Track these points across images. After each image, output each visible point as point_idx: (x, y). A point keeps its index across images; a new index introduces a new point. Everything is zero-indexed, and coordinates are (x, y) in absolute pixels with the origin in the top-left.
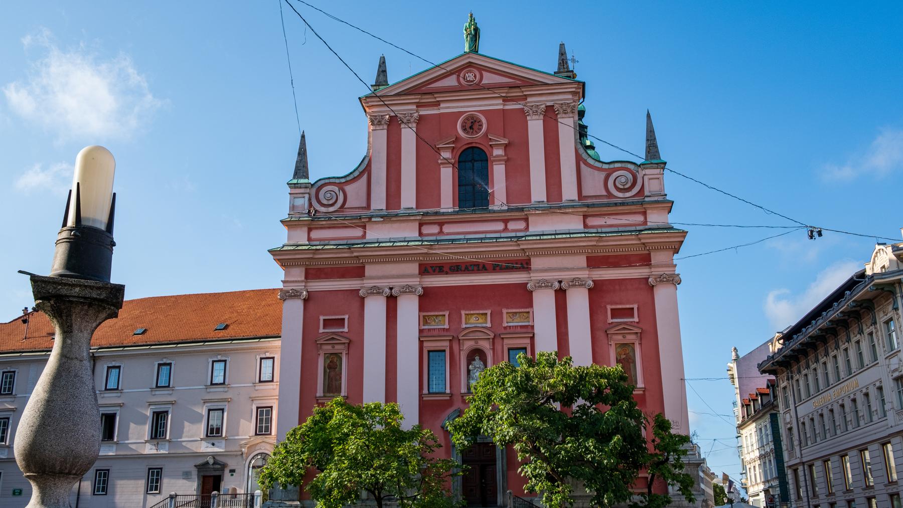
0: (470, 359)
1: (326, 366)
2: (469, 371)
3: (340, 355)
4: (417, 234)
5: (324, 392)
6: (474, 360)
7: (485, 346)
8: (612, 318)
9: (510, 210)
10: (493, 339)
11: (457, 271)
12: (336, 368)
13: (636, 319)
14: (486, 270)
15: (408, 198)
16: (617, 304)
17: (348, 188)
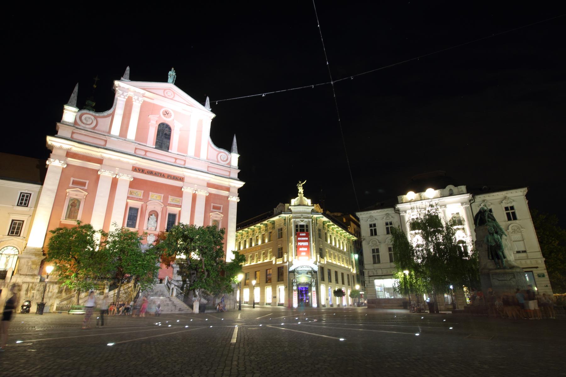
0: (150, 215)
1: (70, 204)
2: (148, 219)
3: (80, 200)
4: (134, 153)
5: (66, 218)
6: (152, 215)
7: (159, 209)
8: (213, 209)
9: (178, 154)
10: (163, 208)
11: (151, 174)
12: (76, 206)
13: (221, 211)
14: (164, 176)
15: (131, 134)
16: (215, 203)
17: (99, 119)
